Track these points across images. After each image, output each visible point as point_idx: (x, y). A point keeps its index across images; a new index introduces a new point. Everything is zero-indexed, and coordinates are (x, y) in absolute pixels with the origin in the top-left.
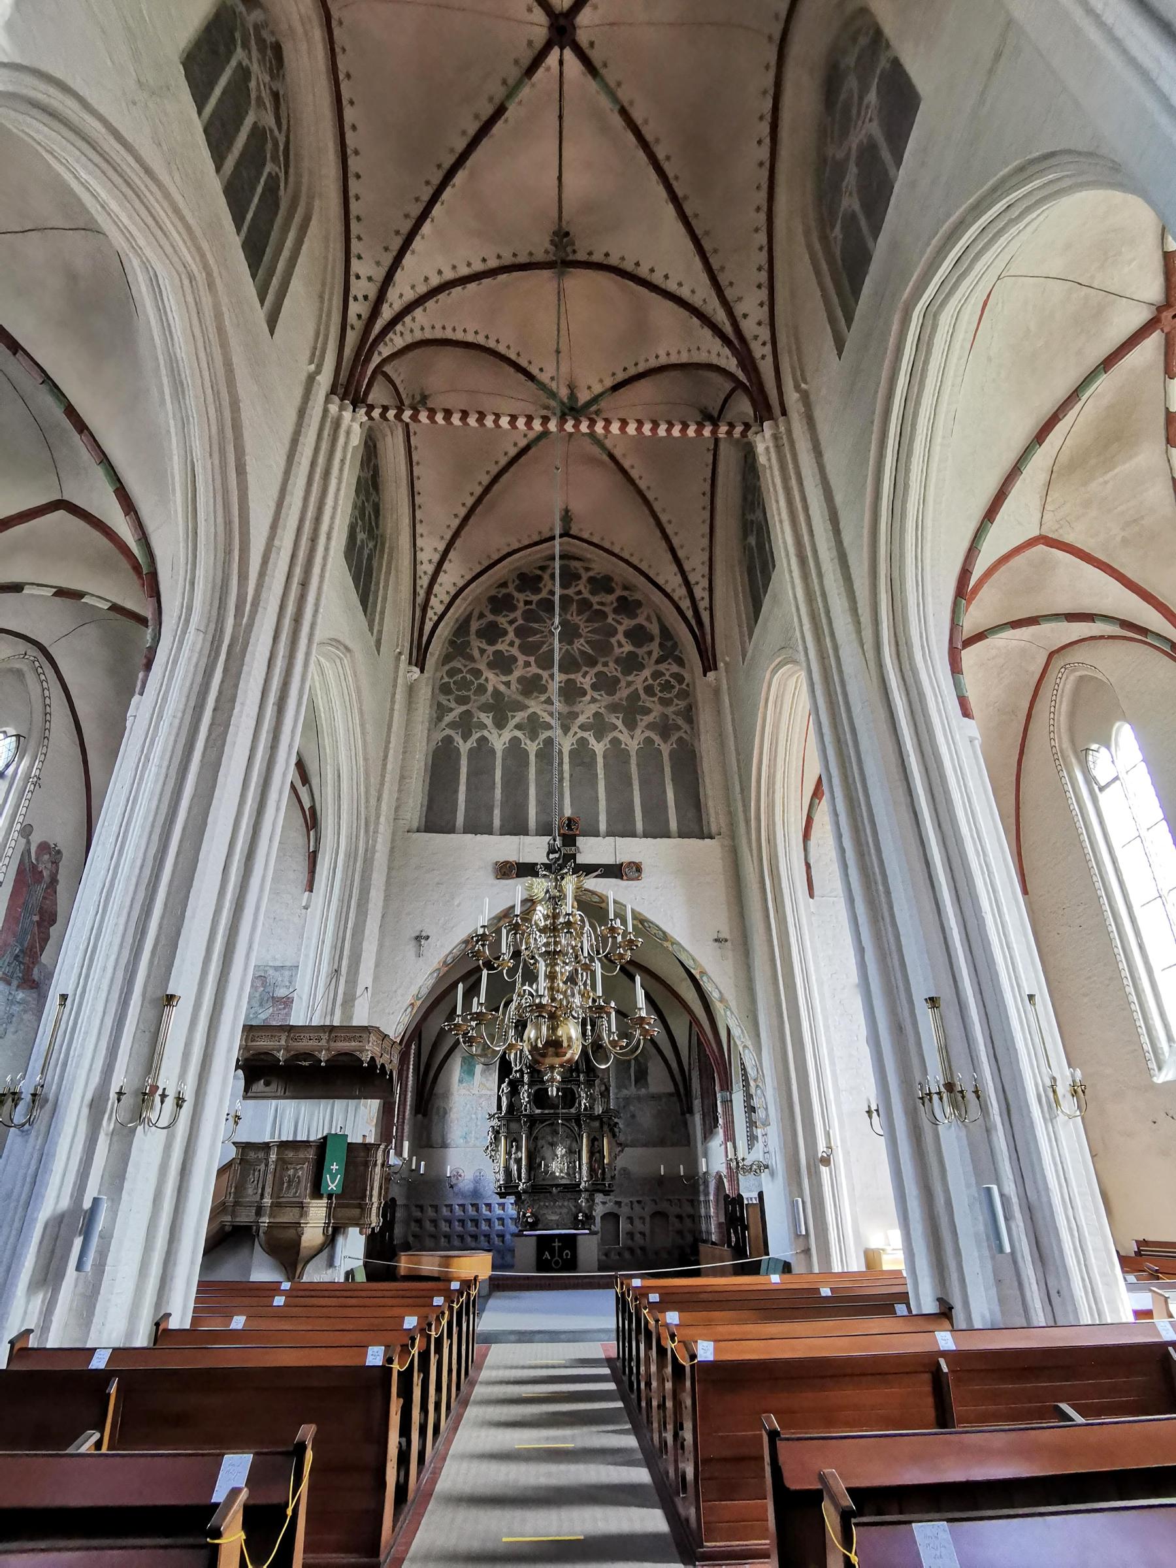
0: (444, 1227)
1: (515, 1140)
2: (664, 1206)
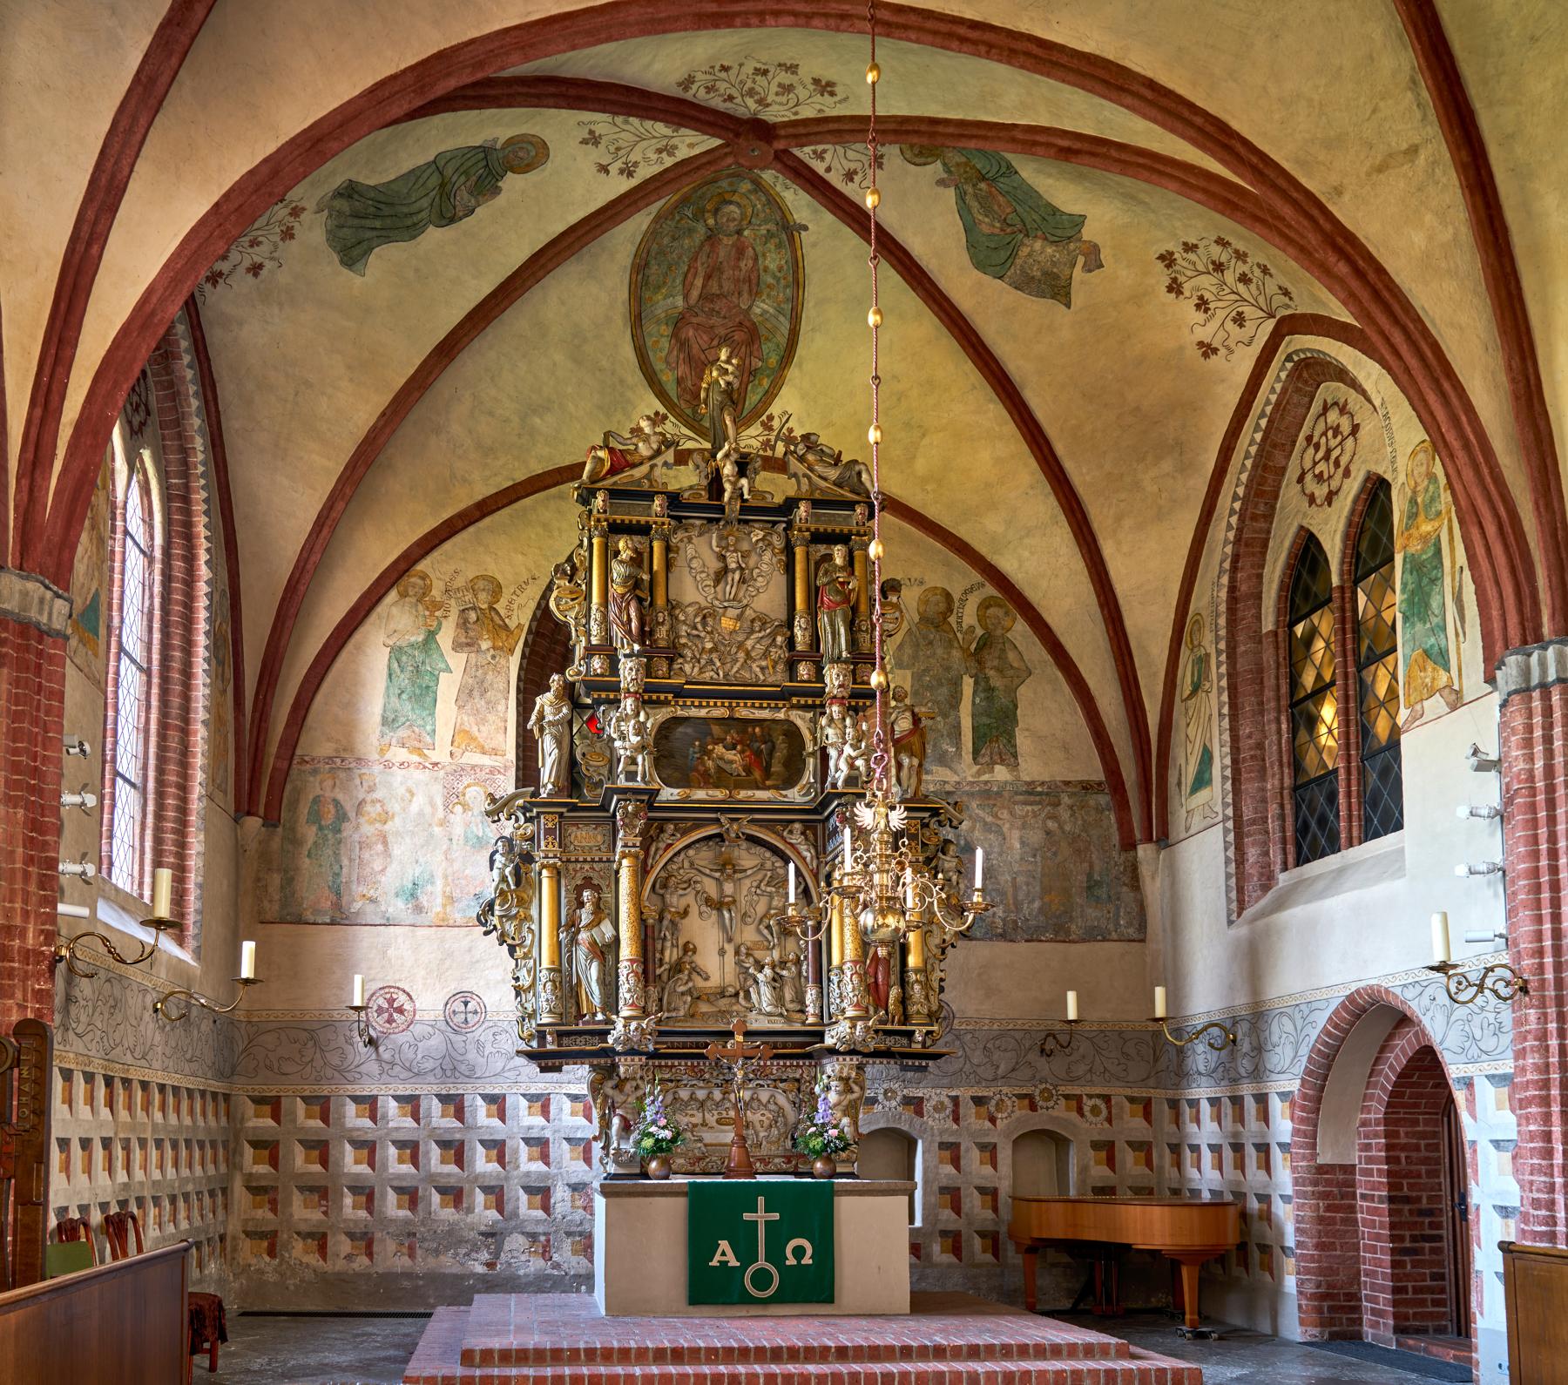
0: (351, 1163)
1: (588, 883)
2: (1057, 1114)
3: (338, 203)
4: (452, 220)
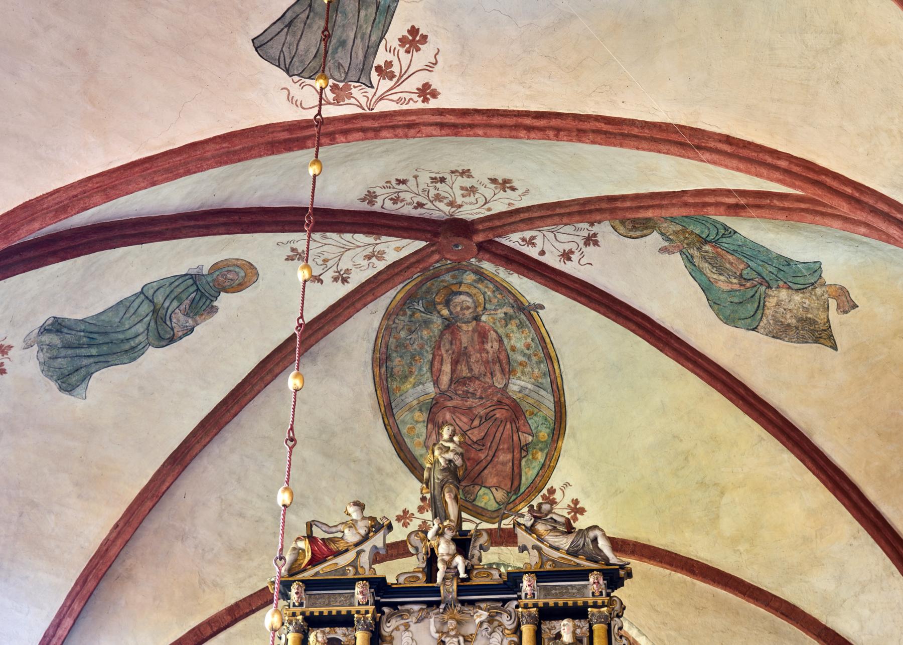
3: (46, 338)
4: (172, 340)
